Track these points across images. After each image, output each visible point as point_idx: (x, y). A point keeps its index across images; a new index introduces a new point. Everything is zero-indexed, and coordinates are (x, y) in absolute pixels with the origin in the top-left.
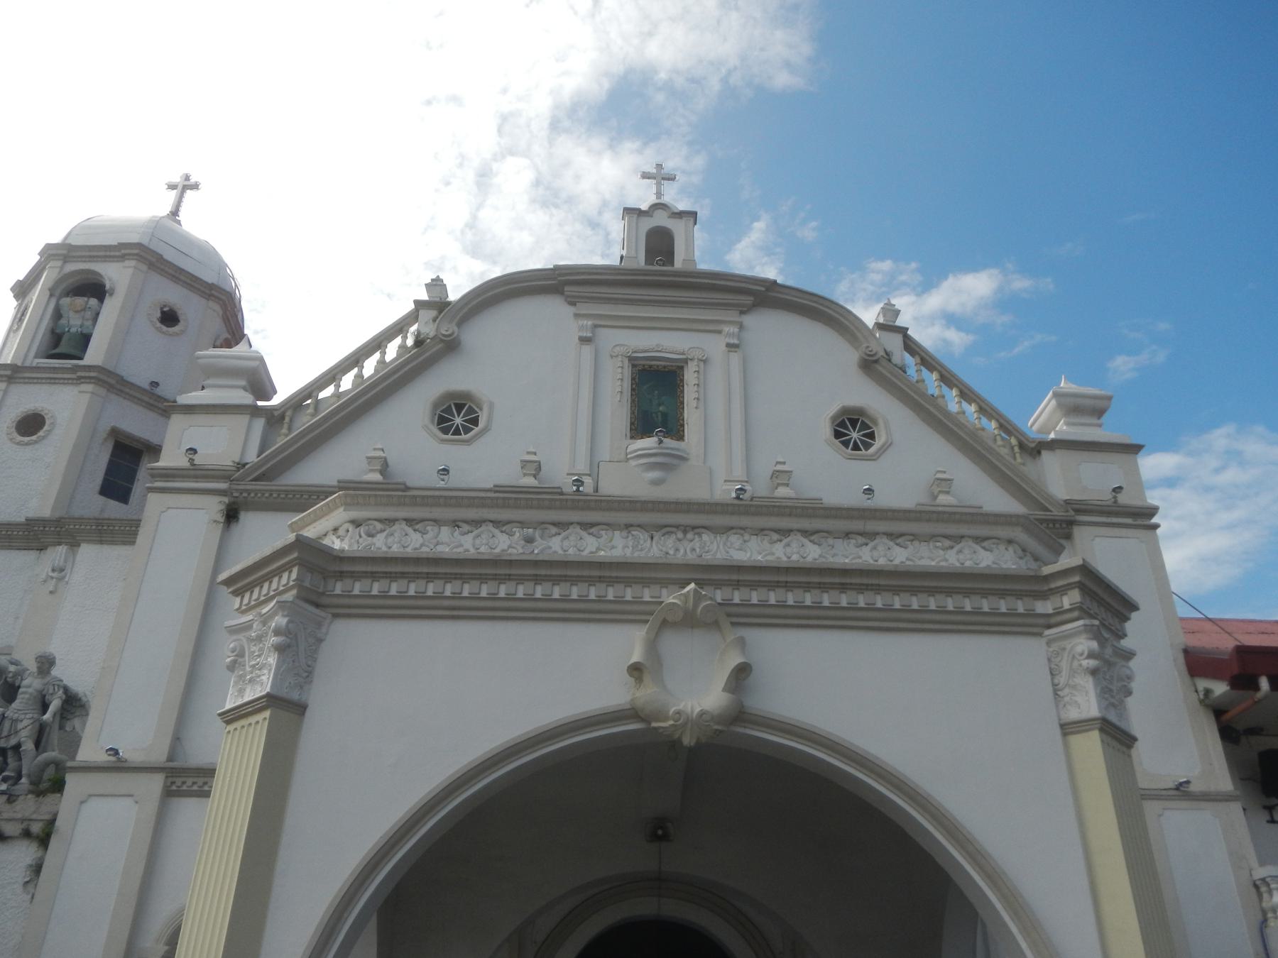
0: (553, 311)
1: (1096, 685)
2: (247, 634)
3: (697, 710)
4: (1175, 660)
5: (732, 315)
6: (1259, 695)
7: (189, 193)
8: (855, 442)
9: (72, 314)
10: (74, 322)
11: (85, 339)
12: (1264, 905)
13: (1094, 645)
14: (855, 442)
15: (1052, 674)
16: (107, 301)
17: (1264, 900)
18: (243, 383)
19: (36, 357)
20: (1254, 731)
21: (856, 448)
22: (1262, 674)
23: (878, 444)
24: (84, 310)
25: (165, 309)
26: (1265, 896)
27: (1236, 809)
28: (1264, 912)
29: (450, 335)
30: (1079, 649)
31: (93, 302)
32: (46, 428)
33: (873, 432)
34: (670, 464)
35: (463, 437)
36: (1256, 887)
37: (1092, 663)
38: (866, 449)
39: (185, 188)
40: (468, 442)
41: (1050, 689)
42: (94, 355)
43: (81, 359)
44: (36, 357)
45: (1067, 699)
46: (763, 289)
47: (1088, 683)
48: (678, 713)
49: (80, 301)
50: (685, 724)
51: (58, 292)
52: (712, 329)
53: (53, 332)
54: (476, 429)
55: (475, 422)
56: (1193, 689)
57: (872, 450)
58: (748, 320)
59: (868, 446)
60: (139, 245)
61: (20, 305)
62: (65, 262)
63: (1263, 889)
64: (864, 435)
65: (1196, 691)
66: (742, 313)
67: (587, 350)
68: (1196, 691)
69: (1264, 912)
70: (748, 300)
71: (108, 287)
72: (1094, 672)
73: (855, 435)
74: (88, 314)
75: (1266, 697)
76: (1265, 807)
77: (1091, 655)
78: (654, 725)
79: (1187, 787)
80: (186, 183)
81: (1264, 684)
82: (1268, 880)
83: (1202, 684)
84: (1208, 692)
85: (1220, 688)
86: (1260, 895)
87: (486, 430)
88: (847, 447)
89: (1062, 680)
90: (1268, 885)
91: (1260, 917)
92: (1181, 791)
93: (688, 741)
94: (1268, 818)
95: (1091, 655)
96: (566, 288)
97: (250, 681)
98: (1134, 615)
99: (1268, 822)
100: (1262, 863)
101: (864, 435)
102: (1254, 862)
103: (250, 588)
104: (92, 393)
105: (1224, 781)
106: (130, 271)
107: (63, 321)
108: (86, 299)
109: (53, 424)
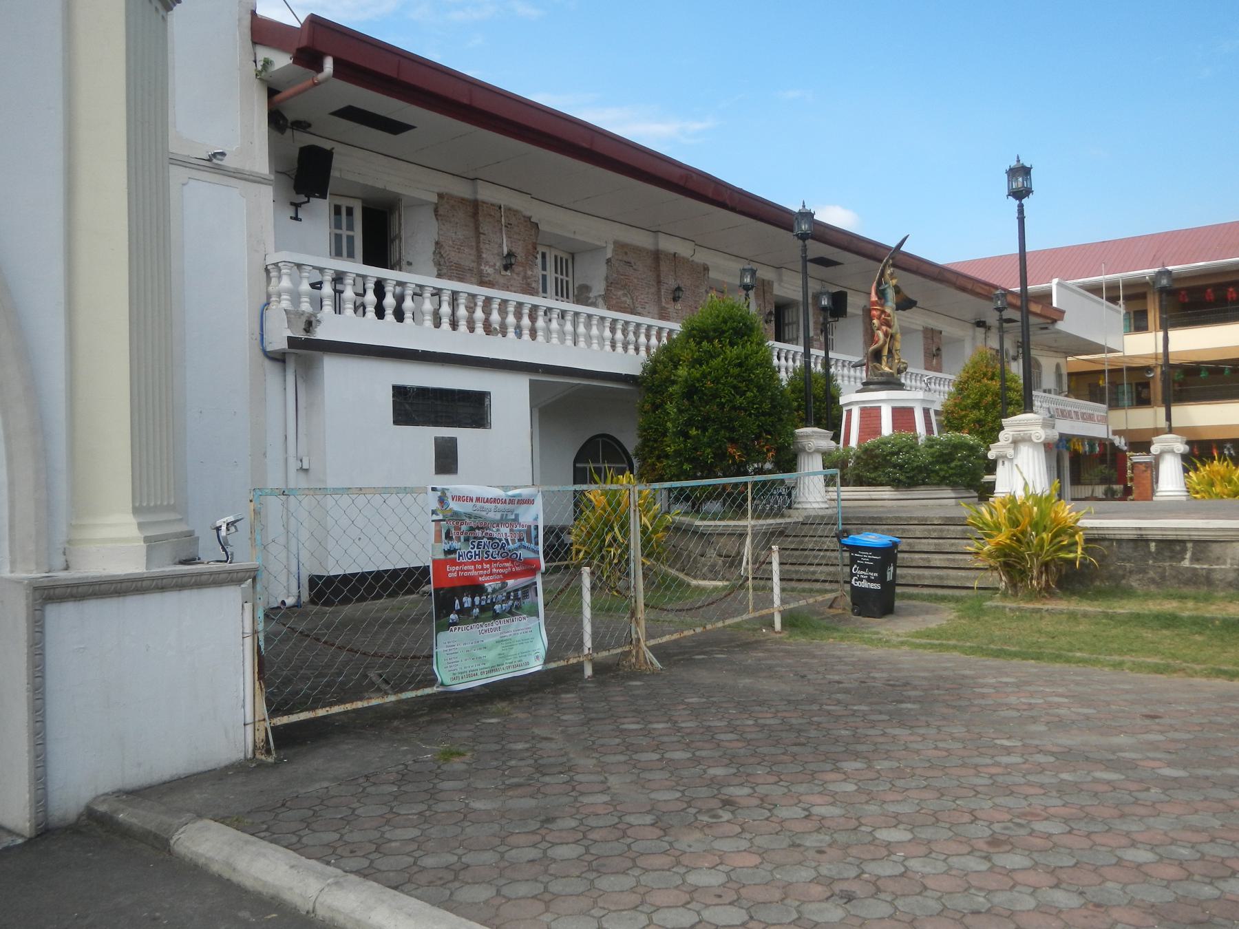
4: (239, 20)
6: (321, 76)
12: (270, 288)
17: (272, 284)
20: (301, 126)
22: (330, 55)
26: (274, 280)
27: (267, 194)
28: (269, 296)
36: (267, 271)
56: (253, 59)
63: (274, 274)
65: (255, 62)
68: (255, 62)
69: (269, 296)
75: (326, 80)
76: (292, 204)
79: (221, 160)
81: (329, 65)
82: (280, 265)
83: (263, 53)
84: (267, 63)
85: (281, 61)
86: (269, 278)
90: (280, 270)
91: (265, 301)
92: (214, 162)
94: (294, 215)
99: (291, 218)
100: (277, 250)
102: (270, 247)
105: (261, 163)
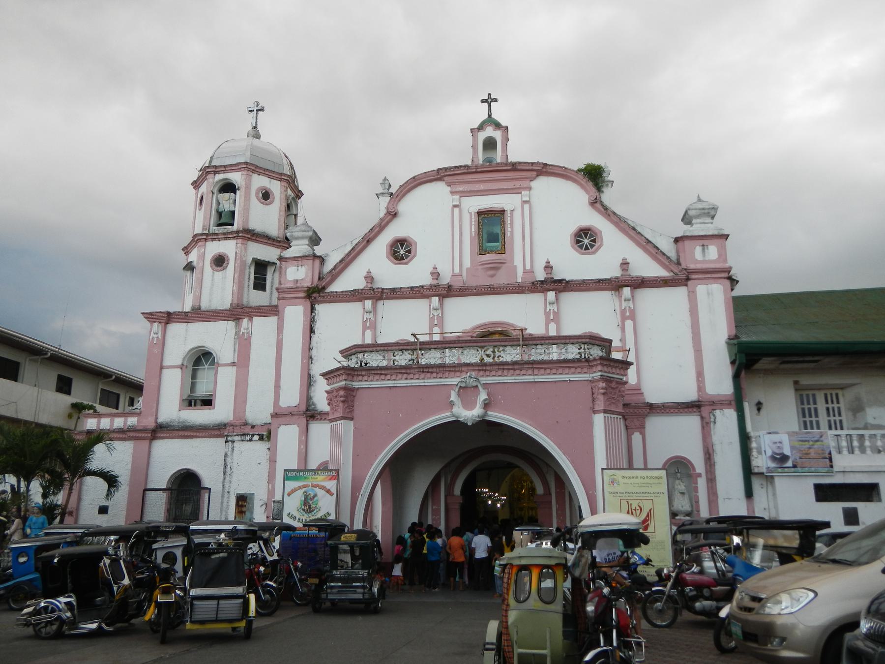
0: (440, 190)
1: (604, 397)
2: (333, 394)
3: (471, 415)
5: (524, 184)
7: (259, 112)
8: (586, 245)
9: (224, 202)
10: (226, 206)
11: (233, 213)
13: (604, 385)
14: (586, 245)
15: (593, 394)
16: (238, 192)
18: (307, 243)
19: (213, 226)
21: (587, 249)
23: (597, 245)
24: (229, 199)
25: (264, 192)
29: (393, 212)
30: (600, 386)
31: (232, 195)
32: (226, 262)
33: (595, 239)
34: (495, 267)
35: (406, 261)
37: (602, 391)
38: (592, 248)
39: (257, 111)
40: (407, 263)
41: (591, 399)
42: (237, 225)
43: (233, 225)
44: (213, 226)
45: (596, 402)
46: (541, 168)
47: (601, 397)
48: (465, 416)
49: (227, 195)
50: (468, 419)
51: (216, 191)
52: (516, 190)
53: (217, 211)
54: (411, 256)
55: (409, 252)
57: (594, 248)
58: (533, 184)
59: (592, 246)
60: (246, 163)
61: (197, 193)
62: (215, 174)
64: (591, 241)
66: (531, 181)
67: (456, 210)
70: (535, 173)
71: (237, 187)
72: (604, 394)
73: (586, 241)
74: (231, 201)
77: (603, 389)
78: (459, 419)
80: (257, 108)
87: (415, 256)
88: (582, 249)
89: (595, 396)
93: (469, 424)
95: (603, 389)
96: (446, 178)
97: (336, 410)
98: (631, 367)
101: (591, 241)
103: (331, 378)
104: (242, 243)
106: (243, 177)
107: (221, 206)
108: (229, 194)
109: (228, 260)
